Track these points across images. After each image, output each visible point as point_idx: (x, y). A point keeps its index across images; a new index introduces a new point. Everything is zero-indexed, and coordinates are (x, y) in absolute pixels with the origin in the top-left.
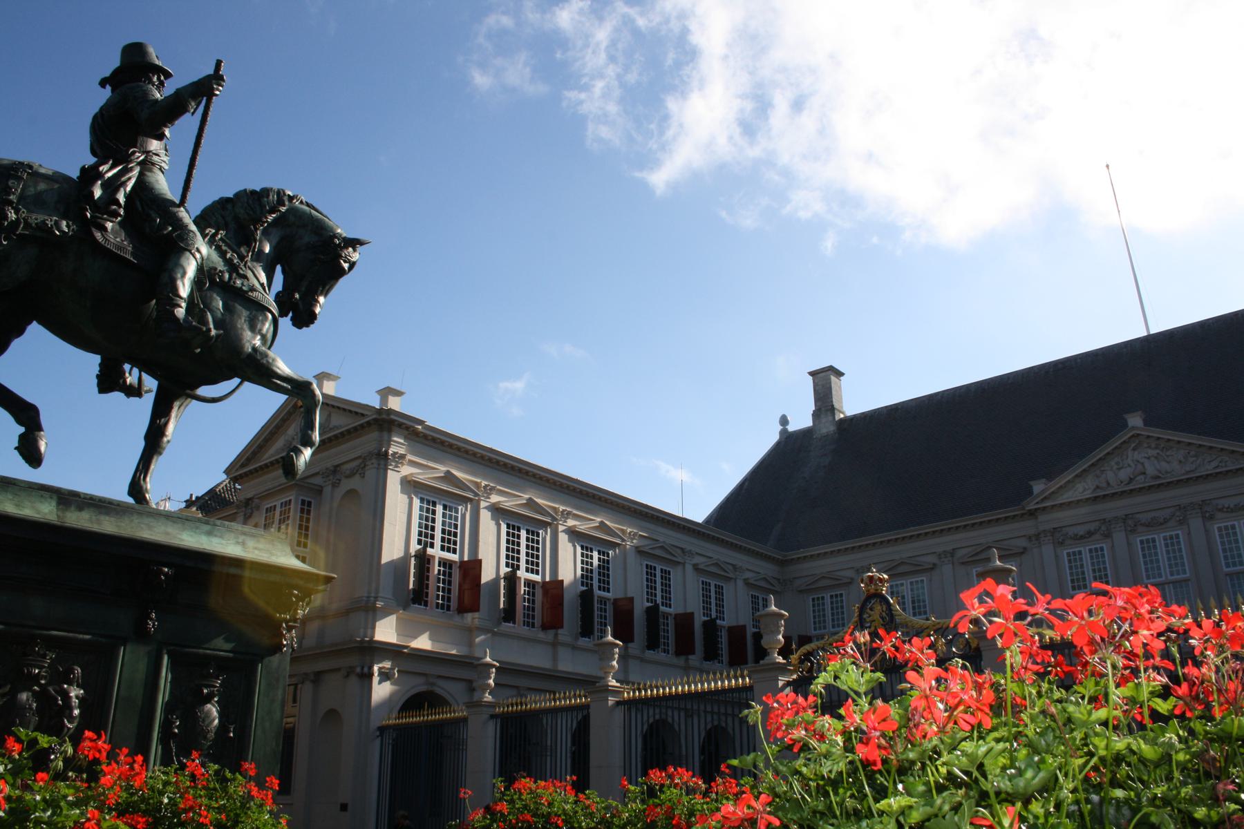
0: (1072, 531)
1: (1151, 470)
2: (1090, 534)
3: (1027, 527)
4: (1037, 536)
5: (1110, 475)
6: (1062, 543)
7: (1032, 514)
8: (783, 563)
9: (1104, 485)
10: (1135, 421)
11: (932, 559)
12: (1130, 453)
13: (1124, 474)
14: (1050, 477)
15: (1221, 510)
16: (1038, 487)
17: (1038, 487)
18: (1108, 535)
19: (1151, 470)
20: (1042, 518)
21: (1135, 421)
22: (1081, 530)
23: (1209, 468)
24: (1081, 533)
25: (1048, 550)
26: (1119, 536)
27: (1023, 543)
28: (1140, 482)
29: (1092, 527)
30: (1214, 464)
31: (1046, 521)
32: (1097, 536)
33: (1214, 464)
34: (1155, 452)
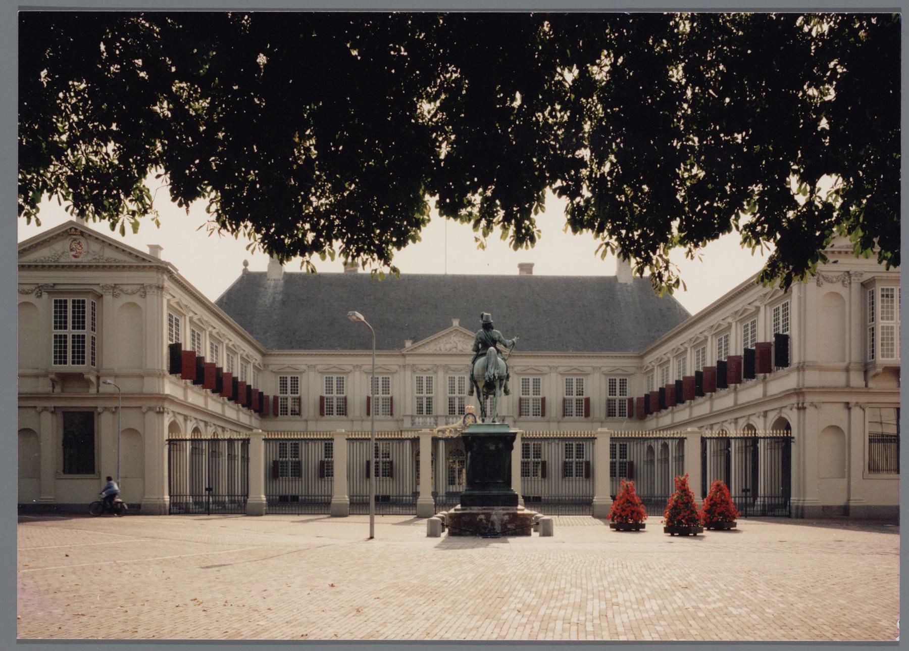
0: (421, 367)
1: (460, 347)
2: (429, 370)
3: (400, 361)
4: (404, 366)
7: (404, 356)
8: (264, 355)
10: (456, 323)
11: (351, 368)
13: (448, 346)
16: (408, 344)
17: (408, 344)
18: (435, 372)
19: (460, 347)
20: (407, 358)
21: (456, 323)
22: (424, 367)
25: (408, 373)
26: (441, 374)
27: (396, 368)
31: (410, 360)
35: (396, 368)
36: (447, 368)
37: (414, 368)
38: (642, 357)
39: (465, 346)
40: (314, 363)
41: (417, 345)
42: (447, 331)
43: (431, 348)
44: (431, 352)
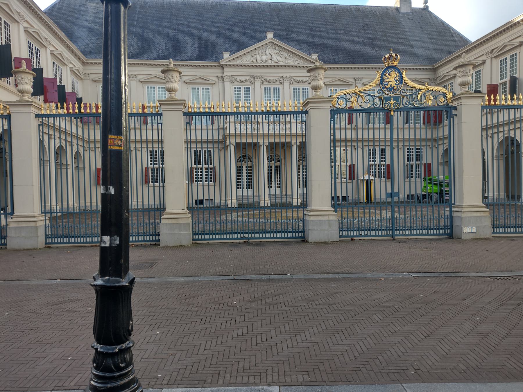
0: (239, 78)
2: (246, 81)
3: (218, 72)
5: (258, 57)
6: (233, 83)
7: (222, 67)
8: (84, 64)
9: (255, 61)
12: (267, 50)
13: (264, 58)
14: (232, 52)
15: (296, 81)
16: (226, 55)
17: (226, 55)
19: (275, 59)
22: (243, 79)
23: (296, 64)
24: (243, 80)
26: (257, 84)
28: (270, 63)
29: (247, 78)
30: (297, 62)
31: (228, 71)
32: (248, 83)
33: (297, 62)
34: (277, 51)
35: (215, 79)
36: (264, 80)
37: (233, 80)
38: (434, 70)
39: (279, 58)
40: (135, 73)
41: (235, 56)
42: (263, 43)
43: (246, 60)
44: (248, 63)
